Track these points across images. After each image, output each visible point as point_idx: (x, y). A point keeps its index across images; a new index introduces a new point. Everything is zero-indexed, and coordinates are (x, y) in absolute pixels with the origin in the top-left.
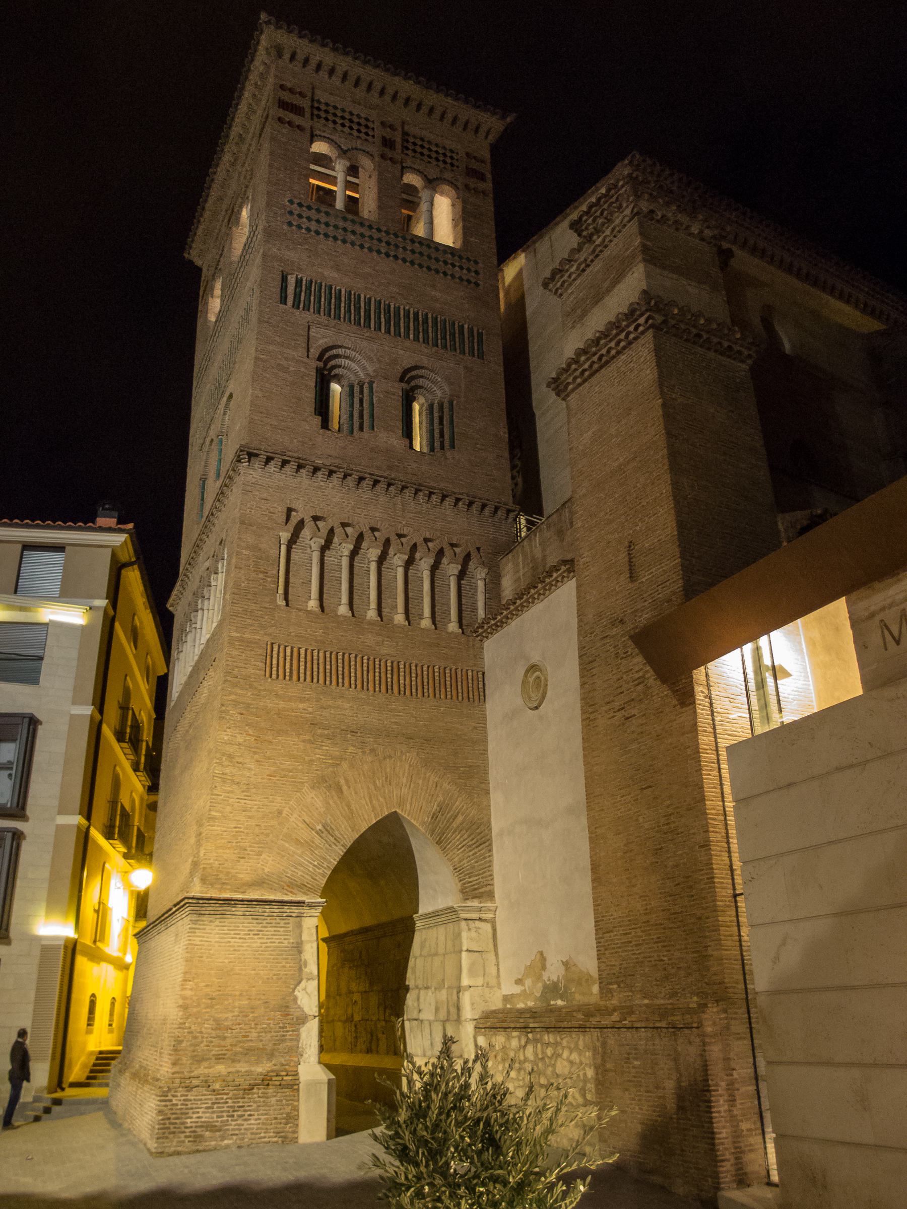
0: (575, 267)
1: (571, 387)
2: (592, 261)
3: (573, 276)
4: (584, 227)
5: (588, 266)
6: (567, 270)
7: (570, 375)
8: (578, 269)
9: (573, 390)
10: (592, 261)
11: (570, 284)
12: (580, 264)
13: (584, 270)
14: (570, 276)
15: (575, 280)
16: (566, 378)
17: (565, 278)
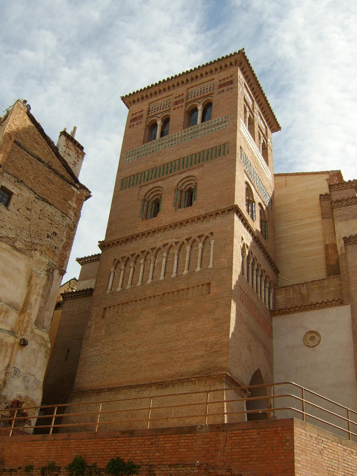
0: (346, 203)
1: (351, 242)
2: (353, 204)
3: (343, 205)
4: (333, 188)
5: (351, 205)
6: (343, 202)
7: (354, 239)
8: (346, 204)
9: (351, 244)
10: (353, 204)
11: (340, 207)
12: (348, 203)
13: (348, 205)
14: (342, 205)
15: (343, 206)
16: (352, 239)
17: (340, 204)
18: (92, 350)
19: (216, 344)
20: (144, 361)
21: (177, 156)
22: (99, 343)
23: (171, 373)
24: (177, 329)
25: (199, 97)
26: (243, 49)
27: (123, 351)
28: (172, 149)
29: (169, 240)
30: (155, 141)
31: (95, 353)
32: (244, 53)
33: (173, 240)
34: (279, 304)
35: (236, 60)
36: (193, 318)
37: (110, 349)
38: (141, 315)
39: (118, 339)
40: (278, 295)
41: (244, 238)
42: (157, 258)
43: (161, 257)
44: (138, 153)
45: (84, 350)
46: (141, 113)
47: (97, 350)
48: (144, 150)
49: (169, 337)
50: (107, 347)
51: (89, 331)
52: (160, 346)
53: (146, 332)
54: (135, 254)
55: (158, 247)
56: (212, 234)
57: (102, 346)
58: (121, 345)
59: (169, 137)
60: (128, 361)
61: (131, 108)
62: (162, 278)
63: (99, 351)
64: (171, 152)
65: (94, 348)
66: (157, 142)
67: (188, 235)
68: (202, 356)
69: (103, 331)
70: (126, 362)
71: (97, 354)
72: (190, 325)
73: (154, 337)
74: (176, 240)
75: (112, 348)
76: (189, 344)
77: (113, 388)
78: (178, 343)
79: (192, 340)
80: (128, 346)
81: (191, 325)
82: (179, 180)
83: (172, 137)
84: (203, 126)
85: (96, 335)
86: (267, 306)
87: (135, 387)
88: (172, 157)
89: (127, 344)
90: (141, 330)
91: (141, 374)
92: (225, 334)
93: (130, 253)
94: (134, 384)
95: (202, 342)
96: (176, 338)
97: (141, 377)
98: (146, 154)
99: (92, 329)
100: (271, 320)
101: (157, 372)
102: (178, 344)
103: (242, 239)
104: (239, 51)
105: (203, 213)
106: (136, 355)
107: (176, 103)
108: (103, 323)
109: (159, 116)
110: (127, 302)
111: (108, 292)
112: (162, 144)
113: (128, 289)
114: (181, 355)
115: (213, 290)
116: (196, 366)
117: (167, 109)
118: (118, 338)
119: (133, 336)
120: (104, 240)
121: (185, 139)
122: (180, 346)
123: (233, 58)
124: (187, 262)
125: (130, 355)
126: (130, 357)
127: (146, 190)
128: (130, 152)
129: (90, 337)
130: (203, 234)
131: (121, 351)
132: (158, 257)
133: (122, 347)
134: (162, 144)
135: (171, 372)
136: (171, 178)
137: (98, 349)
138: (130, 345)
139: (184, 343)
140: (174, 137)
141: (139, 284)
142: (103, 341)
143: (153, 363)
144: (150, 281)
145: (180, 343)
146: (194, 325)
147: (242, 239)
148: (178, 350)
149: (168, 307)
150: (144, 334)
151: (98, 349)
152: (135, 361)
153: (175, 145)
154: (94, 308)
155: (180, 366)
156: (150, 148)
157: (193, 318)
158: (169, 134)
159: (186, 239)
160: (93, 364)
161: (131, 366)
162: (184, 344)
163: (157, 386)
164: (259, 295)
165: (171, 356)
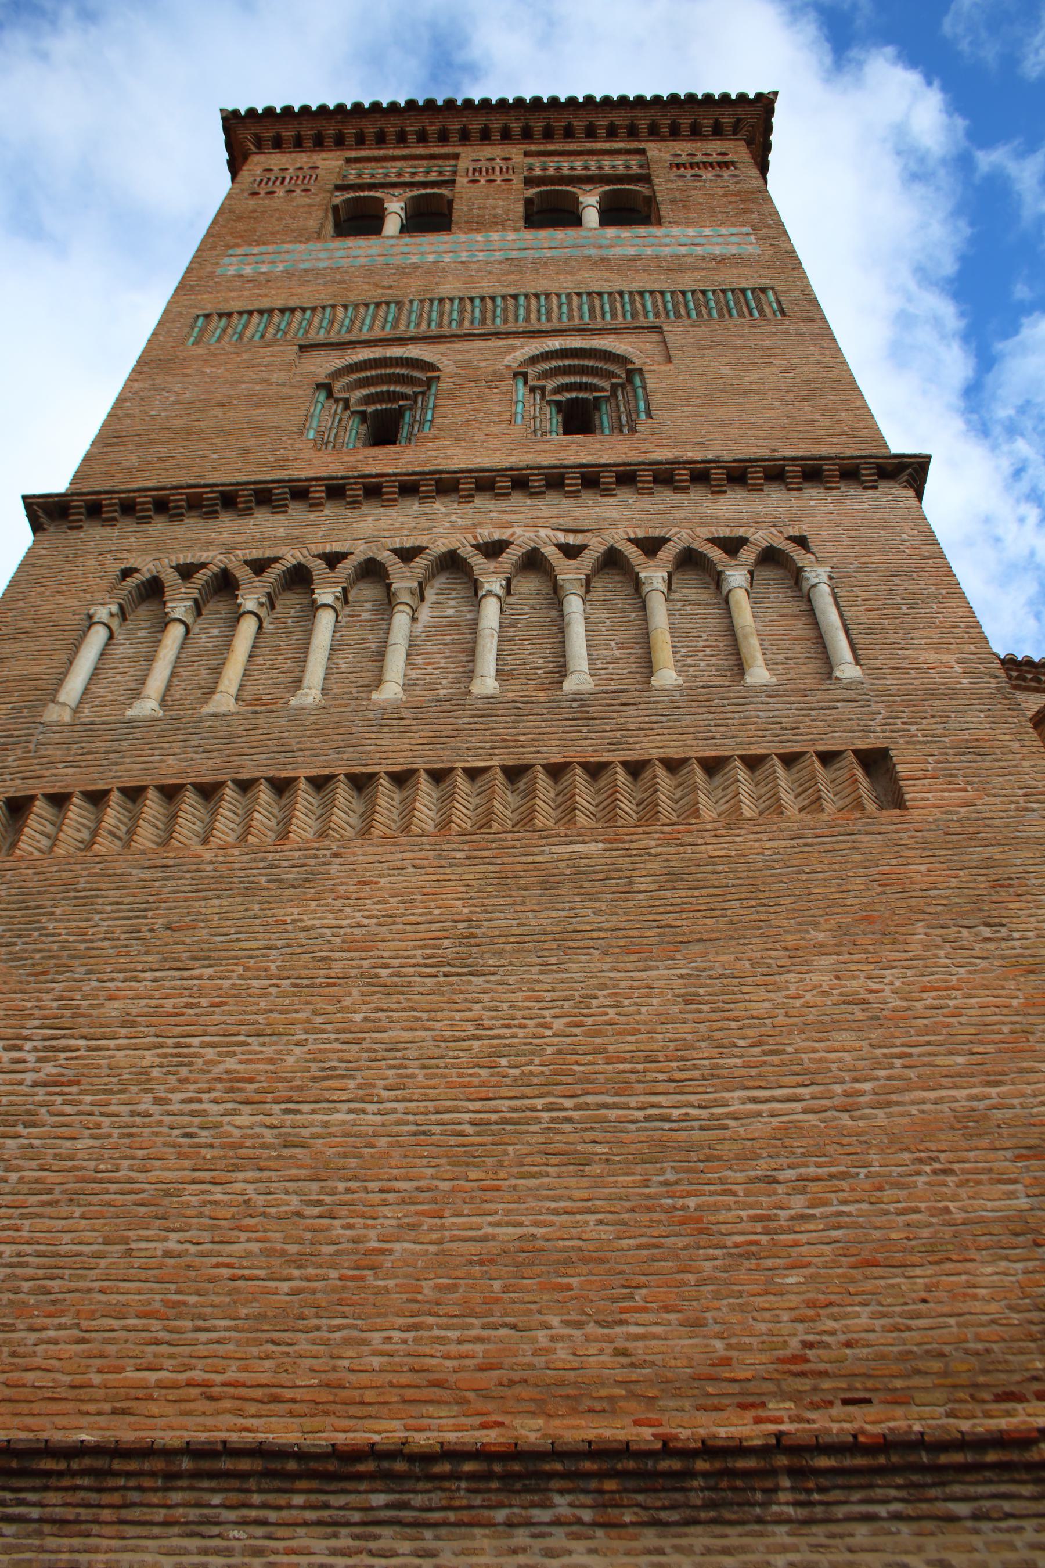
20: (390, 1216)
23: (726, 1362)
26: (776, 93)
27: (158, 1101)
32: (771, 112)
35: (739, 121)
37: (29, 1077)
38: (333, 870)
39: (113, 1009)
42: (427, 604)
43: (452, 603)
49: (629, 1044)
52: (548, 1108)
53: (388, 989)
54: (276, 560)
55: (441, 546)
58: (149, 1057)
61: (257, 164)
62: (487, 683)
72: (815, 977)
73: (470, 1029)
75: (49, 1068)
76: (845, 1119)
77: (49, 1450)
79: (867, 1086)
80: (217, 1070)
81: (826, 980)
87: (332, 1466)
89: (210, 1053)
91: (377, 1336)
93: (238, 552)
94: (282, 1431)
97: (376, 1362)
102: (737, 1107)
104: (759, 96)
111: (54, 714)
114: (798, 1204)
115: (925, 796)
120: (62, 490)
123: (729, 111)
125: (233, 1146)
127: (339, 364)
131: (146, 1104)
132: (430, 594)
138: (231, 1063)
139: (798, 1106)
141: (311, 694)
145: (755, 1100)
148: (748, 1158)
155: (812, 1304)
161: (255, 1247)
163: (610, 1485)
165: (692, 1202)
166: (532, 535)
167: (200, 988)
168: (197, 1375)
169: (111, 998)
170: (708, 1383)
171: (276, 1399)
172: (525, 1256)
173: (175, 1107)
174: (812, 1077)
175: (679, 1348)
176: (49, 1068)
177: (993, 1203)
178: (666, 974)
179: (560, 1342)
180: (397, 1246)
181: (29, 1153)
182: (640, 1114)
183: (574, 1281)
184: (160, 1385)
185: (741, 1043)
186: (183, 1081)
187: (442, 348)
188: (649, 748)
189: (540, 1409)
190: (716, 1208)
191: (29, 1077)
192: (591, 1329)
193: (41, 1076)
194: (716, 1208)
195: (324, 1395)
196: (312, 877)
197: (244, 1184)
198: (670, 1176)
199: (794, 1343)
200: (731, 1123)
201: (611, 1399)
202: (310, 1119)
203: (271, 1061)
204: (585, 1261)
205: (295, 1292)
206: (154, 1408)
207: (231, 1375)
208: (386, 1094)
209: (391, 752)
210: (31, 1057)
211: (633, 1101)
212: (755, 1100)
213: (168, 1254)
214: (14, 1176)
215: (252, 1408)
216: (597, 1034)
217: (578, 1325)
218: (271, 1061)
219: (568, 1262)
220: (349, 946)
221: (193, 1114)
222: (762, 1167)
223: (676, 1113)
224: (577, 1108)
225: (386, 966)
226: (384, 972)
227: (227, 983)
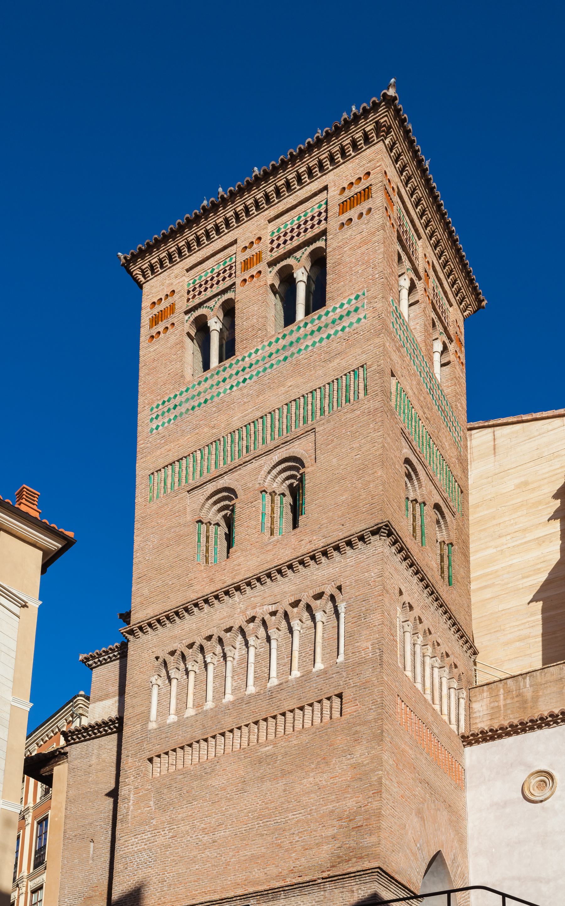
18: (136, 840)
19: (357, 813)
21: (257, 409)
22: (147, 827)
23: (281, 873)
24: (285, 791)
25: (295, 243)
27: (191, 837)
28: (245, 391)
29: (257, 609)
30: (208, 374)
31: (141, 845)
33: (265, 607)
34: (477, 721)
36: (313, 766)
37: (168, 837)
38: (217, 767)
40: (475, 702)
41: (403, 591)
44: (174, 408)
45: (121, 842)
46: (170, 300)
47: (145, 841)
48: (187, 400)
49: (273, 805)
50: (162, 833)
51: (126, 805)
53: (230, 800)
56: (339, 588)
57: (153, 832)
59: (238, 361)
60: (203, 855)
63: (148, 842)
64: (245, 400)
65: (139, 836)
66: (212, 375)
67: (292, 595)
68: (334, 837)
69: (152, 803)
70: (199, 857)
71: (146, 846)
74: (270, 606)
75: (171, 834)
78: (290, 816)
79: (314, 808)
80: (200, 828)
82: (266, 468)
83: (243, 360)
84: (309, 325)
85: (139, 811)
86: (454, 727)
88: (248, 414)
90: (219, 795)
91: (229, 878)
92: (373, 794)
95: (332, 811)
96: (285, 806)
97: (229, 883)
98: (193, 408)
99: (132, 802)
100: (462, 754)
101: (257, 871)
102: (290, 817)
103: (401, 593)
105: (320, 543)
106: (216, 844)
107: (247, 265)
108: (149, 787)
109: (211, 303)
110: (188, 743)
112: (224, 381)
113: (187, 718)
114: (297, 839)
116: (323, 854)
117: (228, 283)
118: (180, 815)
119: (207, 809)
121: (272, 365)
122: (293, 822)
124: (296, 654)
125: (205, 845)
126: (206, 849)
128: (158, 406)
129: (130, 817)
130: (322, 590)
133: (190, 831)
134: (224, 381)
135: (280, 870)
136: (250, 467)
137: (146, 837)
138: (203, 825)
139: (301, 815)
140: (247, 359)
142: (154, 823)
143: (247, 857)
144: (229, 697)
145: (294, 815)
146: (317, 780)
147: (401, 593)
149: (267, 748)
150: (228, 804)
151: (146, 837)
152: (216, 854)
153: (253, 380)
154: (130, 760)
156: (199, 394)
157: (313, 766)
158: (237, 353)
159: (290, 604)
160: (140, 866)
161: (210, 865)
162: (300, 817)
163: (258, 897)
164: (437, 707)
165: (279, 841)
166: (261, 611)
167: (195, 808)
168: (204, 891)
169: (179, 814)
170: (278, 876)
171: (215, 892)
172: (253, 858)
173: (194, 838)
174: (304, 807)
175: (273, 870)
176: (171, 834)
177: (331, 832)
178: (280, 785)
179: (257, 874)
180: (232, 860)
181: (171, 854)
182: (273, 822)
183: (259, 862)
184: (199, 893)
185: (293, 801)
186: (194, 832)
187: (236, 475)
188: (286, 707)
189: (253, 885)
190: (283, 842)
191: (168, 837)
192: (262, 870)
193: (169, 836)
194: (283, 842)
195: (222, 890)
196: (213, 770)
197: (207, 853)
198: (277, 836)
199: (292, 867)
200: (289, 821)
201: (264, 883)
202: (217, 835)
203: (209, 823)
204: (261, 857)
205: (217, 872)
206: (198, 897)
207: (209, 889)
208: (229, 827)
209: (229, 722)
210: (167, 832)
211: (272, 819)
212: (294, 815)
213: (197, 869)
214: (169, 859)
215: (212, 894)
216: (267, 803)
217: (259, 870)
218: (209, 823)
219: (258, 858)
220: (223, 789)
221: (197, 839)
222: (292, 831)
223: (279, 821)
224: (263, 823)
225: (228, 794)
226: (228, 795)
227: (199, 805)
